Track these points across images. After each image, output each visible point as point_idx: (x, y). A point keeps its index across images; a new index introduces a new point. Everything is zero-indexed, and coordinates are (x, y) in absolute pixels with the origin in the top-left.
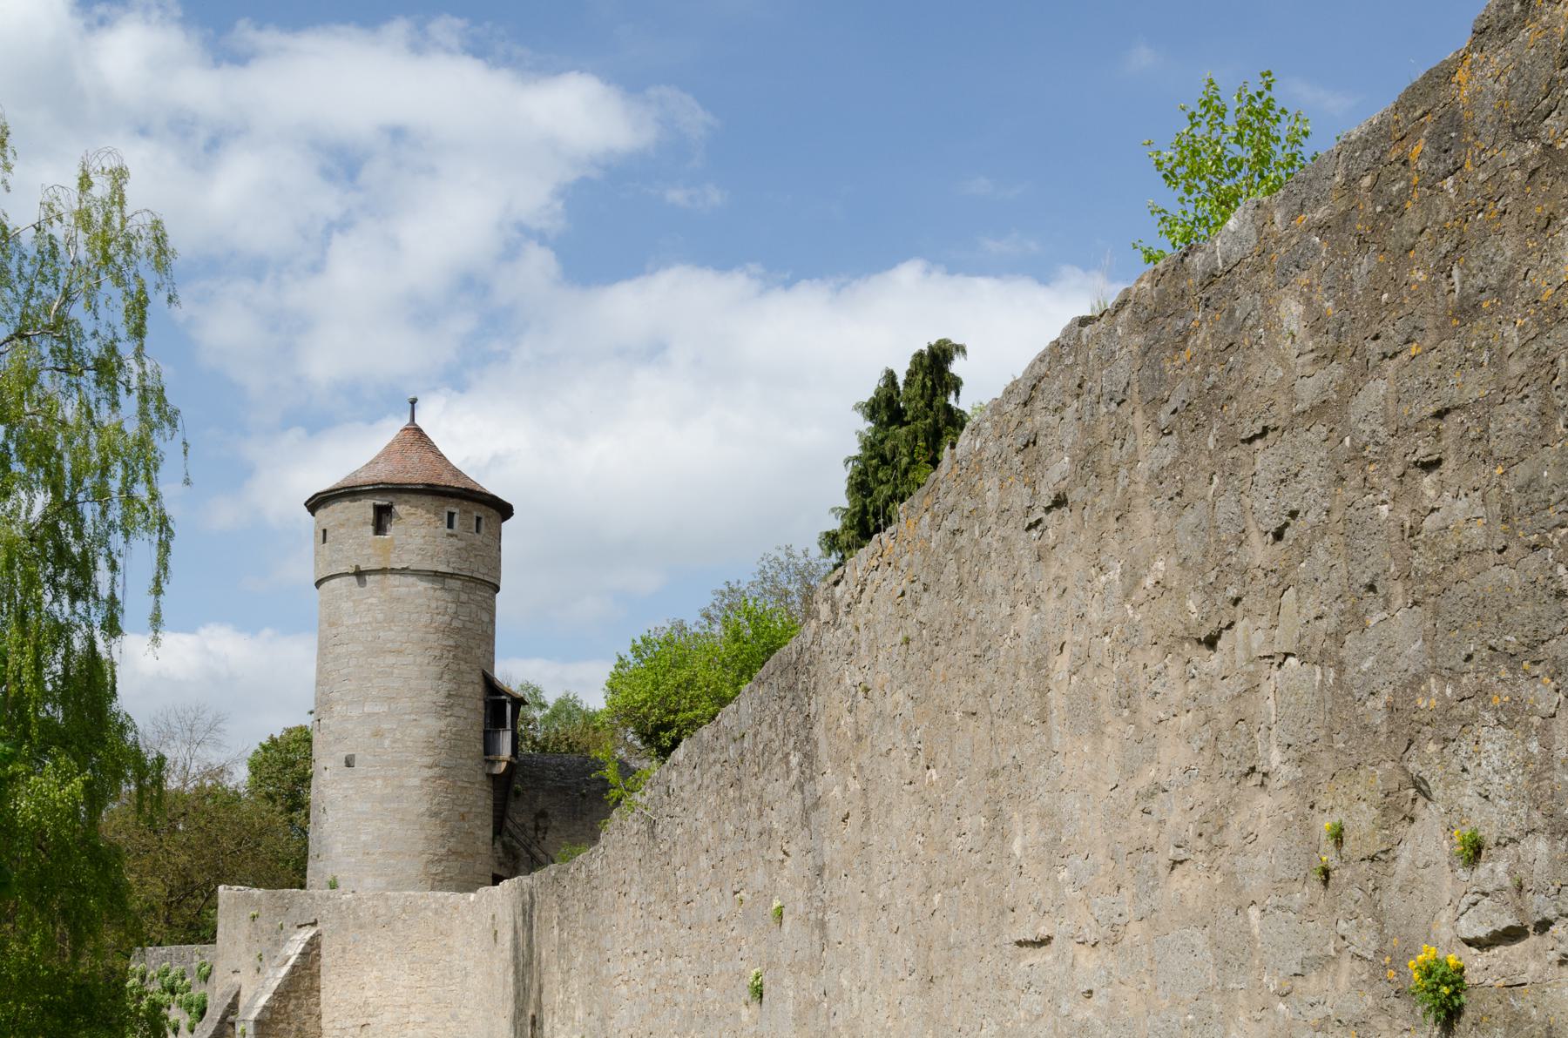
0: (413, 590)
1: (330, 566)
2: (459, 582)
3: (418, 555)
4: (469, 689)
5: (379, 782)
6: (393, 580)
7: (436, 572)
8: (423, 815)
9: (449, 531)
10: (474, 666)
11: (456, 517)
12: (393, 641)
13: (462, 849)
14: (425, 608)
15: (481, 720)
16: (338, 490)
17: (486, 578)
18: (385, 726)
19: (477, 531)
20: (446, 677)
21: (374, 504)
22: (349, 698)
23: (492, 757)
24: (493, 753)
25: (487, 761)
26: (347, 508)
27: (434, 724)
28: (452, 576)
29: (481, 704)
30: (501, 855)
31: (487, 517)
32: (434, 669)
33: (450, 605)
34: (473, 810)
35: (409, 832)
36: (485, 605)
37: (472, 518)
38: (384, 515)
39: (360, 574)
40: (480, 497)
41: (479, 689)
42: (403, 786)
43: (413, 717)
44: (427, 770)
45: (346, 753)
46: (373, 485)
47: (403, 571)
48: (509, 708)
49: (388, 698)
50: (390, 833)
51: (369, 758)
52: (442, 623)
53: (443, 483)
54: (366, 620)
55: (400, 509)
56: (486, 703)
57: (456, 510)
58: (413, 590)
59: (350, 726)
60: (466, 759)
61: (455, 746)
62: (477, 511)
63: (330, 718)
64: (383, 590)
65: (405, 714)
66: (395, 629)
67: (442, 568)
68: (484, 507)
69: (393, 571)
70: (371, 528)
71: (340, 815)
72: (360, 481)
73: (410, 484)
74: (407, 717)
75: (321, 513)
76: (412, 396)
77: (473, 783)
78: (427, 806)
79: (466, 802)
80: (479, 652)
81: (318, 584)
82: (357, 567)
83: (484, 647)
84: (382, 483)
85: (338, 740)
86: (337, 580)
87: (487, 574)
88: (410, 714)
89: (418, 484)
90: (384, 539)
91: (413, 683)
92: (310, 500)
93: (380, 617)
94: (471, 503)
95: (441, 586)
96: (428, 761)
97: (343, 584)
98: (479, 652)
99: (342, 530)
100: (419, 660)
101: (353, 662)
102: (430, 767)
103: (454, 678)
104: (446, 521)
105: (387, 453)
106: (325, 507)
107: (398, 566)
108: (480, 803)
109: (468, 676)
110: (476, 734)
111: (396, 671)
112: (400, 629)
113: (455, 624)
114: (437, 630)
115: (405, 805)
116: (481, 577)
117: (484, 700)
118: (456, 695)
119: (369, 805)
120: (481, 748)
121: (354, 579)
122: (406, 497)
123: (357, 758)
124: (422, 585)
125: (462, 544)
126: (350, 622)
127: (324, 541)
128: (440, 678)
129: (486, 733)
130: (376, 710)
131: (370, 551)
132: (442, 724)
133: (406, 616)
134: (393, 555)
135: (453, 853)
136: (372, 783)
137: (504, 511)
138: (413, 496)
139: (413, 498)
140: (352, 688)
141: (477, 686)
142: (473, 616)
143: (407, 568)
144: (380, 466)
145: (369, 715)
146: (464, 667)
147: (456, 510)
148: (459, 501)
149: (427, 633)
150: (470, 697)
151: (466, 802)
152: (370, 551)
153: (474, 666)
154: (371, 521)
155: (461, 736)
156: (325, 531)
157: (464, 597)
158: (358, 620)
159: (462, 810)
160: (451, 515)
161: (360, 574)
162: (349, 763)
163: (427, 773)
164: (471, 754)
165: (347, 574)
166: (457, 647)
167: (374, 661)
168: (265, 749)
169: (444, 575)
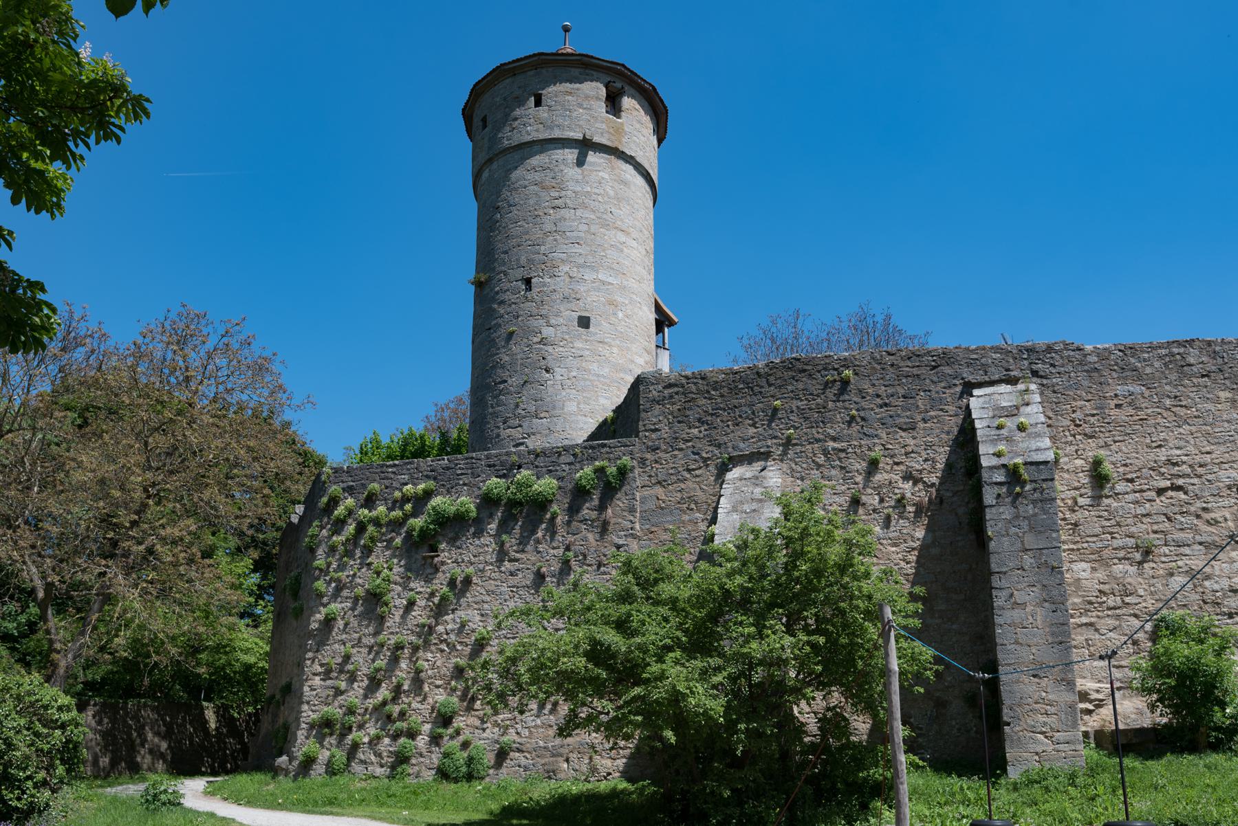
5: (615, 350)
6: (621, 164)
7: (649, 174)
22: (581, 261)
45: (579, 314)
47: (630, 160)
54: (597, 191)
64: (613, 168)
71: (574, 374)
73: (642, 79)
93: (612, 193)
99: (570, 98)
130: (610, 280)
140: (581, 251)
145: (604, 283)
152: (604, 126)
158: (589, 189)
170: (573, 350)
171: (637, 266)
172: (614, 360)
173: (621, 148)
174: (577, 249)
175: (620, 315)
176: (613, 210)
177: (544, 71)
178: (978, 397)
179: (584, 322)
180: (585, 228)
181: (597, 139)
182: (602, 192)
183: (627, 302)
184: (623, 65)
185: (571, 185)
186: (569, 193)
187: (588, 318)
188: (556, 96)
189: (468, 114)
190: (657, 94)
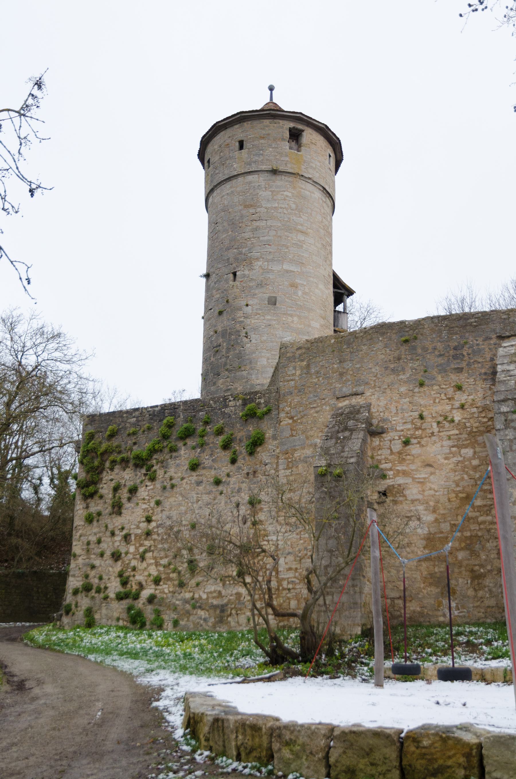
1: (250, 165)
5: (296, 319)
6: (301, 184)
7: (324, 189)
12: (302, 225)
18: (298, 281)
42: (309, 326)
45: (268, 295)
51: (288, 301)
54: (283, 206)
63: (249, 270)
64: (294, 188)
66: (303, 217)
71: (265, 338)
74: (311, 279)
85: (260, 285)
86: (256, 176)
93: (293, 206)
99: (262, 141)
101: (272, 233)
111: (304, 246)
112: (307, 218)
123: (278, 299)
126: (269, 205)
130: (292, 268)
131: (287, 159)
133: (309, 211)
134: (303, 167)
136: (290, 319)
140: (270, 250)
143: (310, 178)
145: (287, 271)
152: (287, 159)
158: (276, 205)
167: (290, 235)
170: (265, 322)
171: (314, 257)
173: (301, 173)
174: (269, 249)
175: (300, 293)
176: (294, 218)
177: (245, 124)
178: (505, 347)
179: (273, 302)
180: (274, 233)
181: (281, 168)
182: (287, 206)
183: (305, 283)
184: (301, 113)
185: (264, 204)
186: (263, 210)
187: (275, 298)
188: (253, 141)
189: (201, 156)
190: (330, 130)
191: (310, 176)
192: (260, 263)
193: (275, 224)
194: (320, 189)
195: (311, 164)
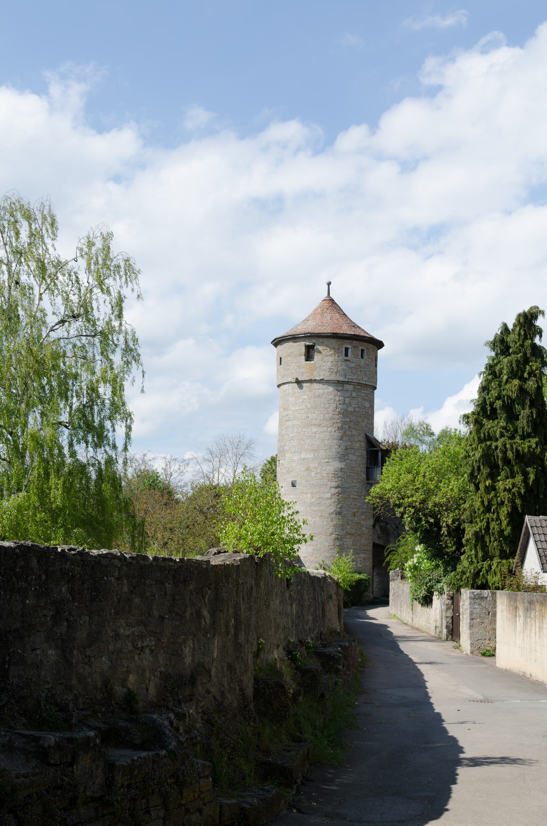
0: (326, 391)
1: (284, 377)
2: (352, 386)
3: (328, 372)
4: (358, 445)
5: (309, 495)
6: (315, 386)
7: (339, 381)
8: (332, 513)
9: (346, 358)
10: (361, 432)
11: (350, 350)
12: (316, 419)
13: (354, 532)
14: (332, 401)
15: (365, 461)
16: (286, 336)
17: (367, 383)
18: (312, 465)
19: (362, 357)
20: (345, 439)
21: (305, 345)
22: (293, 450)
23: (370, 482)
24: (371, 479)
25: (368, 483)
26: (291, 346)
27: (337, 465)
28: (348, 383)
29: (365, 452)
30: (379, 533)
31: (368, 349)
32: (338, 434)
33: (346, 399)
34: (360, 510)
35: (325, 523)
36: (367, 398)
37: (358, 351)
38: (311, 350)
39: (298, 382)
40: (363, 339)
41: (364, 444)
43: (327, 460)
44: (334, 489)
45: (292, 479)
46: (304, 334)
48: (380, 454)
49: (313, 450)
50: (315, 523)
52: (342, 409)
53: (342, 332)
54: (302, 408)
55: (319, 347)
56: (367, 452)
57: (350, 346)
58: (326, 391)
59: (294, 465)
60: (356, 483)
61: (350, 476)
62: (362, 346)
64: (310, 391)
65: (322, 459)
66: (317, 412)
67: (341, 379)
68: (365, 344)
69: (315, 381)
70: (303, 358)
72: (298, 332)
73: (323, 333)
74: (323, 460)
75: (279, 347)
76: (328, 282)
77: (360, 496)
78: (334, 509)
79: (356, 506)
80: (363, 424)
81: (279, 386)
82: (297, 379)
83: (366, 421)
84: (309, 333)
86: (287, 385)
87: (368, 381)
88: (325, 459)
89: (328, 333)
90: (311, 364)
91: (327, 442)
92: (273, 341)
94: (358, 342)
95: (341, 388)
96: (334, 484)
97: (290, 388)
98: (363, 424)
99: (289, 359)
100: (329, 429)
102: (336, 488)
103: (349, 439)
104: (344, 352)
105: (314, 313)
106: (281, 345)
107: (318, 378)
108: (364, 507)
109: (357, 437)
110: (361, 469)
111: (317, 435)
113: (350, 409)
114: (339, 413)
115: (323, 508)
116: (364, 383)
117: (367, 450)
118: (350, 449)
119: (304, 508)
120: (364, 476)
121: (296, 385)
122: (322, 340)
123: (298, 482)
124: (331, 389)
125: (353, 365)
126: (294, 409)
127: (281, 364)
128: (341, 440)
129: (367, 468)
130: (307, 456)
131: (303, 370)
132: (342, 465)
134: (315, 372)
135: (349, 534)
137: (379, 345)
138: (326, 339)
139: (326, 341)
141: (362, 443)
142: (360, 404)
143: (323, 379)
144: (309, 322)
145: (304, 459)
146: (354, 432)
147: (350, 346)
148: (351, 341)
149: (334, 414)
150: (358, 449)
151: (356, 506)
152: (303, 370)
153: (361, 432)
154: (304, 354)
155: (353, 470)
156: (281, 358)
157: (354, 394)
158: (298, 408)
159: (354, 510)
160: (347, 349)
161: (298, 382)
162: (293, 485)
163: (334, 491)
164: (358, 480)
165: (291, 382)
166: (350, 422)
167: (307, 430)
168: (269, 462)
169: (343, 383)
172: (308, 501)
183: (317, 466)
186: (290, 412)
191: (322, 378)
192: (288, 455)
193: (297, 423)
194: (334, 383)
195: (323, 368)
